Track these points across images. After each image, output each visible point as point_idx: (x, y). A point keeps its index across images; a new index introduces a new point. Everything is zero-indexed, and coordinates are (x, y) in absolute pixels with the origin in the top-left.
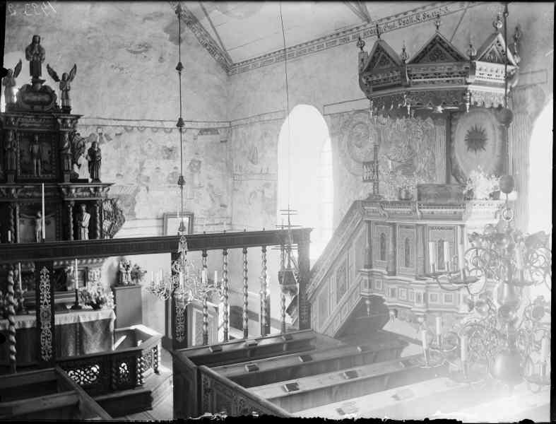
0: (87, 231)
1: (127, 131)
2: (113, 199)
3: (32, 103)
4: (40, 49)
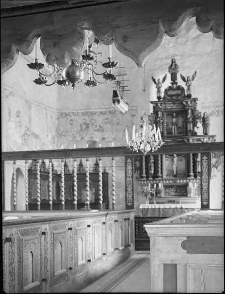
3: (171, 96)
4: (176, 65)
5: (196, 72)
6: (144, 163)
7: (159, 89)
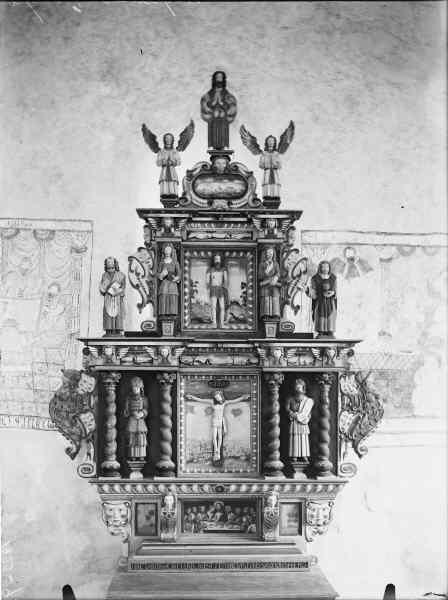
0: (306, 430)
1: (403, 254)
2: (360, 372)
3: (211, 198)
5: (292, 126)
6: (113, 421)
7: (168, 165)
